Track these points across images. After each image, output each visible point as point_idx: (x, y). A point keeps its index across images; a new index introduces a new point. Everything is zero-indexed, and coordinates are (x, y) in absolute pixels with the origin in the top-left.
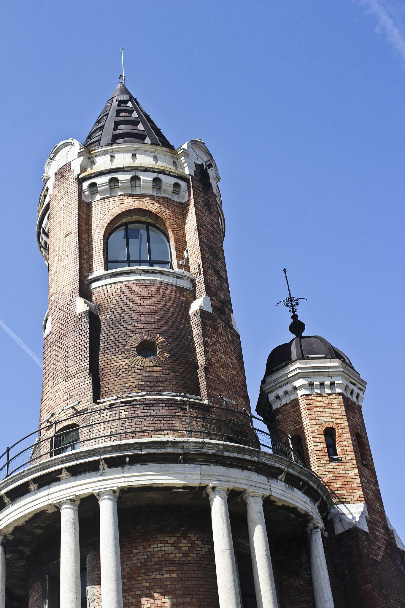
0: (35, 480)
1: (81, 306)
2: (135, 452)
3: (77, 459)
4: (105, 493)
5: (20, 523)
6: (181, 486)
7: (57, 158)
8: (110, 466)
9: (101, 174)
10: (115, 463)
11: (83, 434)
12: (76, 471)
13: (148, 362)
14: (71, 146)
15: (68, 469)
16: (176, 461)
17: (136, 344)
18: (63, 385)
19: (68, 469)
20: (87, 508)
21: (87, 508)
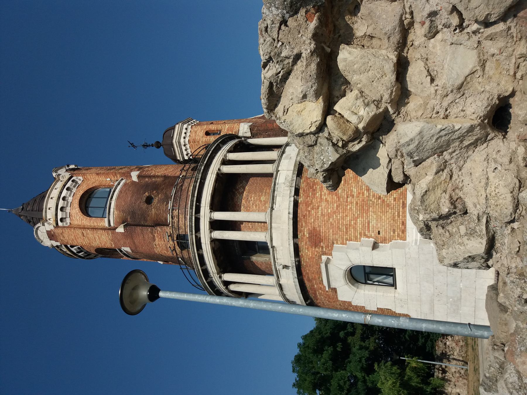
4: (211, 215)
5: (216, 262)
10: (198, 210)
11: (182, 232)
12: (198, 229)
13: (155, 201)
15: (196, 232)
18: (157, 242)
19: (196, 233)
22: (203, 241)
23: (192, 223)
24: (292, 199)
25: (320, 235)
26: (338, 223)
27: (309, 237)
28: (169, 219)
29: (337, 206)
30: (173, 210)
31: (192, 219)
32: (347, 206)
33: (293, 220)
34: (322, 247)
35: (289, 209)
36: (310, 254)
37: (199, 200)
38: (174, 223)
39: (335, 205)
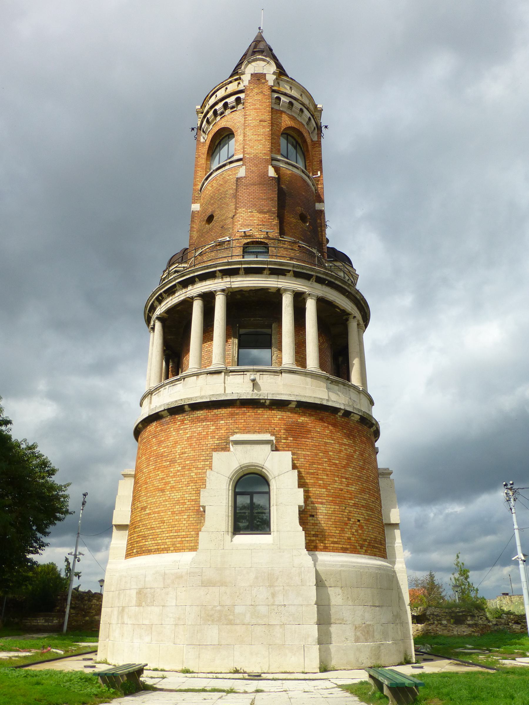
1: (272, 173)
2: (333, 280)
3: (303, 269)
4: (314, 296)
6: (342, 308)
7: (253, 64)
8: (316, 281)
9: (285, 94)
14: (266, 63)
19: (294, 272)
20: (299, 300)
21: (299, 300)
23: (307, 270)
24: (342, 407)
25: (303, 437)
26: (319, 464)
28: (287, 238)
29: (336, 464)
31: (312, 271)
32: (338, 476)
33: (321, 404)
34: (286, 439)
35: (332, 401)
36: (276, 421)
37: (331, 285)
38: (284, 244)
39: (337, 462)
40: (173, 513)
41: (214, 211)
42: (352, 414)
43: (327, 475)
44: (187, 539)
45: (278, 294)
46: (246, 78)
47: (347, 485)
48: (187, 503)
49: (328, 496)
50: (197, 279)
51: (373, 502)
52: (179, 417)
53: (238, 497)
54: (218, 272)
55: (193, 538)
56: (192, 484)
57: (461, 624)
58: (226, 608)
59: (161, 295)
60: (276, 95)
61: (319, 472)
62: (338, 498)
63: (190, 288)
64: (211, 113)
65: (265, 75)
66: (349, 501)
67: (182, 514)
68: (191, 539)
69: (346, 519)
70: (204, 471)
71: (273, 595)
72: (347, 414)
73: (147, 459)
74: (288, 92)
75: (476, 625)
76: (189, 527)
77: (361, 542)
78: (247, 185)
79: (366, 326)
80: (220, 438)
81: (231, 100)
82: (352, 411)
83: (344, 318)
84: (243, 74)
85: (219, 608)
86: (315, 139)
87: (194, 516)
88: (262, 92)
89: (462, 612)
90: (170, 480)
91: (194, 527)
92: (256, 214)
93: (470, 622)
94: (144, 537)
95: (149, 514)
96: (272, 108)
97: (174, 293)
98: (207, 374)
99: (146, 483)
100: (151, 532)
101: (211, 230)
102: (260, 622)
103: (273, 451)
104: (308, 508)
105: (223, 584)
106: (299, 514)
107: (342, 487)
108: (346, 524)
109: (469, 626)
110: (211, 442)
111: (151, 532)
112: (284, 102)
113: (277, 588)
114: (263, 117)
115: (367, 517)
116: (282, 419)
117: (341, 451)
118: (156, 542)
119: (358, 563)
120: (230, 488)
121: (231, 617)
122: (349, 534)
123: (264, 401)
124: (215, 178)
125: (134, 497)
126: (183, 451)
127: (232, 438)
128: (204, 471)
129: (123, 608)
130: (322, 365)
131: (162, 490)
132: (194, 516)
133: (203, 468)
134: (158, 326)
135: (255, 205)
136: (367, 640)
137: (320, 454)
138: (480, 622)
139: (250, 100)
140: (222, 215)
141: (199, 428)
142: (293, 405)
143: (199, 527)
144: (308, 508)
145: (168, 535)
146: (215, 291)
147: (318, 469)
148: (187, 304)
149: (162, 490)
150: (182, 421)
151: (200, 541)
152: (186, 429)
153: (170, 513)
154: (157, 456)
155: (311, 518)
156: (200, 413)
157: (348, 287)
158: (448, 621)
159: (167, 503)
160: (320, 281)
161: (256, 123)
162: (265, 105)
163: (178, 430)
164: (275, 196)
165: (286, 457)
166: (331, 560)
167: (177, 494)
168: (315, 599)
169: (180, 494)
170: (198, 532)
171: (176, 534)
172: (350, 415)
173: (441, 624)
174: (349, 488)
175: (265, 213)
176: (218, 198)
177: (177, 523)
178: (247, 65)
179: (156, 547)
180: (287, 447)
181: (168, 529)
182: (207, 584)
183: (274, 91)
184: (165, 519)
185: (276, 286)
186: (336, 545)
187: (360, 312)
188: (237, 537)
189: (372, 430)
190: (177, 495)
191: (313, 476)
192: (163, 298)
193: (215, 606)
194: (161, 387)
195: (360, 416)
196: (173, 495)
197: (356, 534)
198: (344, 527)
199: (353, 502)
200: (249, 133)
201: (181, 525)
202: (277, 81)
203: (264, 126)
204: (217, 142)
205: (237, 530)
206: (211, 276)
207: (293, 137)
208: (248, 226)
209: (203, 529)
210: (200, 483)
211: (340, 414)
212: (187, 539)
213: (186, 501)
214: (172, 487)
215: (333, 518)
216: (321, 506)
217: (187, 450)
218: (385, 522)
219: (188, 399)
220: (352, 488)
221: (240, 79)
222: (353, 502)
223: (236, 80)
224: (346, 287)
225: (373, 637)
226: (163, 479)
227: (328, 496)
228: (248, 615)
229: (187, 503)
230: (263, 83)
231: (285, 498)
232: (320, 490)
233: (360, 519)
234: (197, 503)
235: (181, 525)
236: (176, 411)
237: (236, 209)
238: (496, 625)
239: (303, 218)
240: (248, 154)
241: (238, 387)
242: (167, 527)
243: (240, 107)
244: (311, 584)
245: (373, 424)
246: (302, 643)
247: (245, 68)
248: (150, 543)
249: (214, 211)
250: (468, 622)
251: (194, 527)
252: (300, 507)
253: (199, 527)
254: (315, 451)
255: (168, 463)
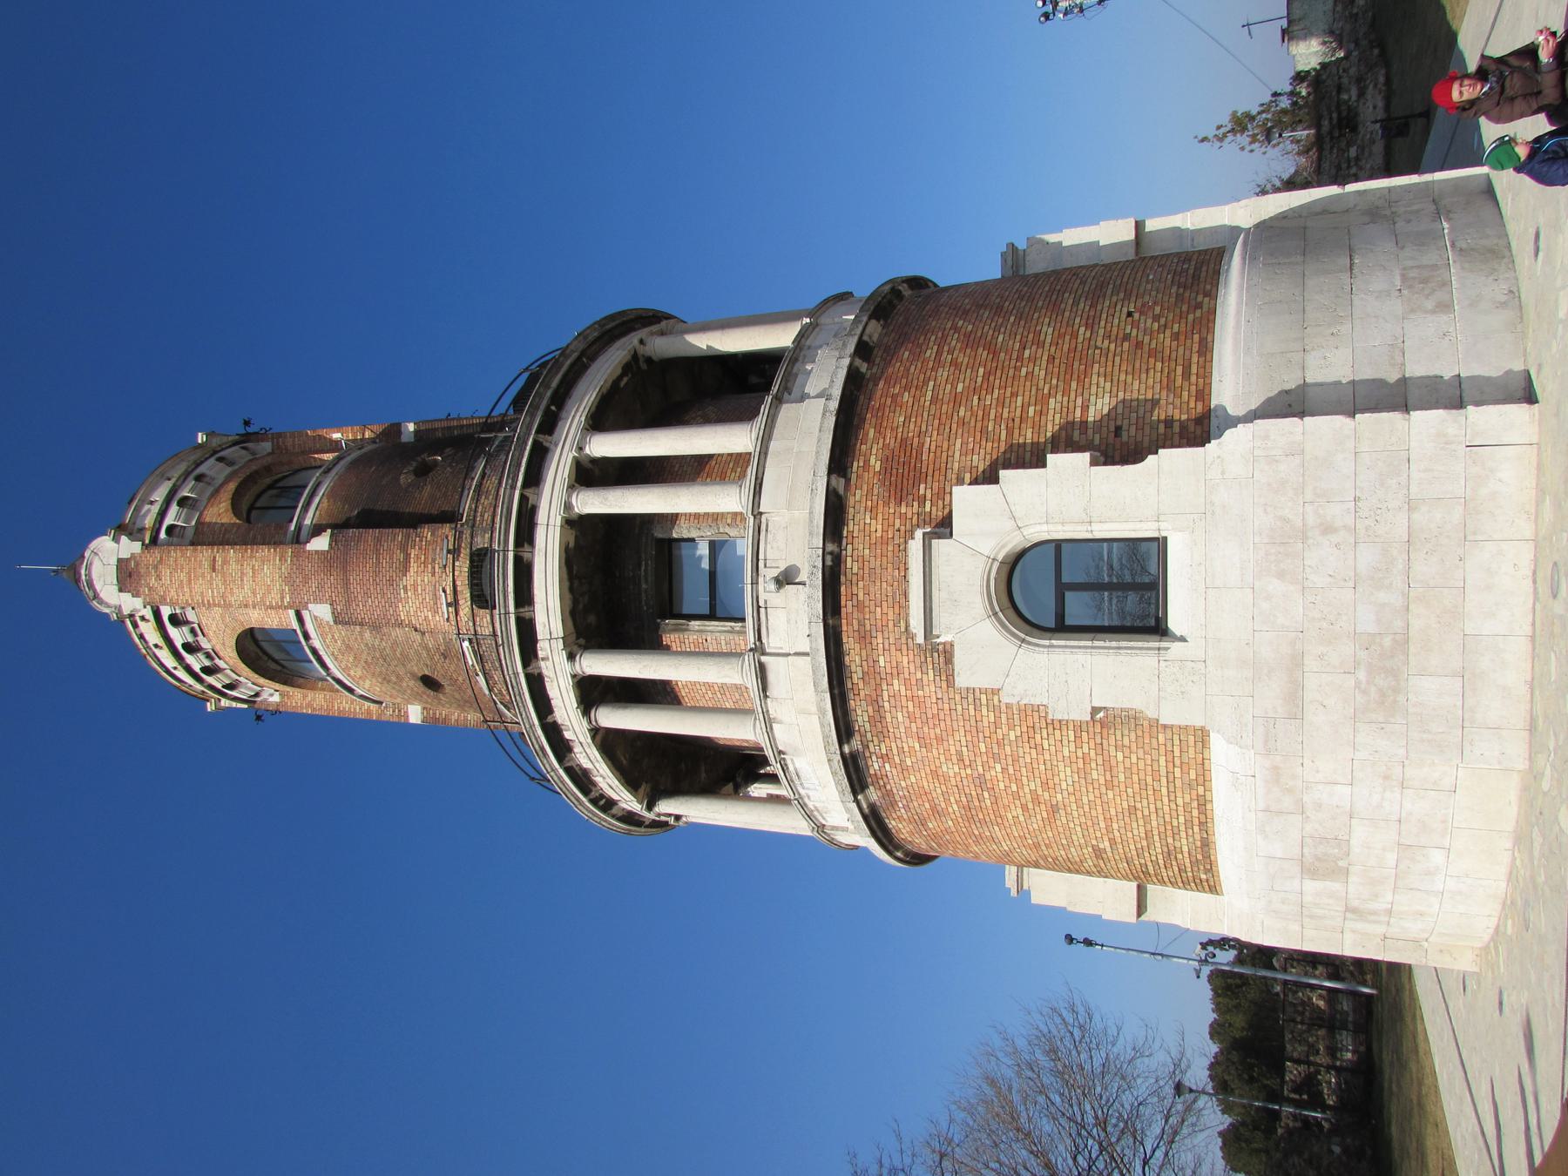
0: (518, 544)
1: (321, 543)
2: (549, 393)
3: (519, 465)
6: (619, 371)
7: (98, 587)
9: (162, 514)
16: (585, 368)
17: (411, 478)
19: (524, 486)
20: (591, 474)
21: (591, 474)
22: (541, 517)
24: (847, 361)
26: (986, 415)
27: (886, 471)
28: (467, 505)
30: (483, 476)
34: (922, 500)
39: (981, 370)
40: (1109, 785)
41: (413, 675)
42: (865, 338)
43: (1014, 395)
44: (1177, 753)
45: (578, 525)
46: (129, 603)
47: (1040, 344)
48: (1086, 750)
49: (1066, 392)
50: (550, 719)
51: (1083, 283)
52: (875, 766)
53: (1069, 621)
54: (530, 670)
55: (1176, 738)
56: (1038, 737)
57: (1357, 114)
58: (1362, 654)
59: (594, 802)
60: (163, 535)
61: (1005, 415)
62: (1074, 368)
63: (568, 735)
64: (210, 680)
65: (120, 561)
66: (1080, 339)
67: (1113, 763)
68: (1177, 742)
69: (1126, 345)
70: (1003, 708)
71: (1328, 529)
72: (863, 350)
73: (977, 842)
74: (155, 509)
75: (1359, 80)
76: (1147, 748)
77: (1185, 308)
78: (348, 602)
79: (668, 317)
80: (922, 667)
81: (178, 636)
82: (855, 339)
83: (644, 366)
84: (119, 609)
85: (1362, 675)
86: (267, 446)
87: (1118, 733)
88: (156, 567)
89: (1330, 113)
90: (1027, 790)
91: (1147, 735)
92: (409, 579)
93: (1354, 92)
94: (1169, 854)
95: (1112, 842)
96: (192, 544)
97: (586, 772)
98: (766, 697)
99: (1037, 846)
100: (1156, 838)
101: (454, 682)
102: (1400, 565)
103: (951, 535)
104: (1097, 442)
105: (1296, 662)
106: (1114, 464)
107: (1045, 358)
108: (1139, 345)
109: (1361, 94)
110: (931, 688)
111: (1156, 838)
112: (178, 517)
113: (1311, 520)
114: (206, 564)
115: (1122, 295)
116: (873, 510)
117: (955, 364)
118: (1182, 828)
119: (1238, 313)
120: (1047, 642)
121: (1387, 641)
122: (1166, 339)
123: (829, 558)
124: (346, 670)
125: (1070, 871)
126: (954, 759)
127: (920, 639)
128: (1003, 708)
129: (1348, 909)
130: (745, 415)
131: (1054, 809)
132: (1118, 733)
133: (996, 709)
134: (667, 807)
135: (391, 582)
136: (1446, 284)
137: (962, 413)
138: (1353, 71)
139: (173, 593)
140: (419, 656)
141: (897, 719)
142: (839, 484)
143: (1146, 723)
144: (1097, 442)
145: (1166, 800)
146: (574, 676)
147: (999, 418)
148: (609, 742)
149: (1054, 809)
150: (885, 758)
151: (1183, 723)
152: (901, 750)
153: (1110, 794)
154: (971, 819)
155: (1124, 434)
156: (861, 714)
157: (567, 357)
158: (1349, 145)
159: (1085, 800)
160: (550, 425)
161: (218, 581)
162: (181, 561)
163: (904, 770)
164: (372, 534)
165: (967, 500)
166: (1233, 380)
167: (1062, 775)
168: (1339, 421)
169: (1061, 768)
170: (1155, 725)
171: (1164, 780)
172: (866, 343)
173: (1357, 159)
174: (1049, 340)
175: (407, 556)
176: (383, 663)
177: (1135, 778)
178: (101, 602)
179: (1196, 829)
180: (943, 495)
181: (1152, 799)
182: (1295, 699)
183: (155, 540)
184: (1125, 805)
185: (558, 529)
186: (1194, 369)
187: (634, 330)
188: (1174, 623)
189: (906, 291)
190: (1066, 776)
191: (1016, 431)
192: (602, 796)
193: (1357, 685)
194: (803, 806)
195: (870, 318)
196: (1064, 786)
197: (1163, 321)
198: (1146, 348)
199: (1082, 329)
200: (238, 596)
201: (1141, 765)
202: (134, 532)
203: (225, 562)
204: (273, 666)
205: (1156, 627)
206: (537, 685)
207: (259, 496)
208: (435, 597)
209: (1151, 713)
210: (1034, 720)
211: (864, 367)
212: (1177, 753)
213: (1080, 754)
214: (1045, 785)
215: (1123, 377)
216: (1092, 409)
217: (952, 749)
218: (1131, 256)
219: (827, 744)
220: (1048, 332)
221: (131, 616)
222: (1082, 329)
223: (135, 626)
224: (569, 362)
225: (1435, 267)
226: (1024, 808)
227: (1066, 392)
228: (1382, 596)
229: (1086, 750)
230: (137, 564)
231: (1070, 499)
232: (1051, 412)
233: (1125, 310)
234: (1084, 727)
235: (1141, 765)
236: (856, 774)
237: (401, 624)
238: (1357, 43)
239: (424, 471)
240: (282, 598)
241: (792, 621)
242: (1145, 803)
243: (191, 616)
244: (1299, 430)
245: (893, 289)
246: (1461, 450)
247: (108, 606)
248: (1184, 841)
249: (413, 675)
250: (1354, 98)
251: (1147, 735)
252: (1094, 463)
253: (1146, 723)
254: (954, 426)
255: (986, 794)
